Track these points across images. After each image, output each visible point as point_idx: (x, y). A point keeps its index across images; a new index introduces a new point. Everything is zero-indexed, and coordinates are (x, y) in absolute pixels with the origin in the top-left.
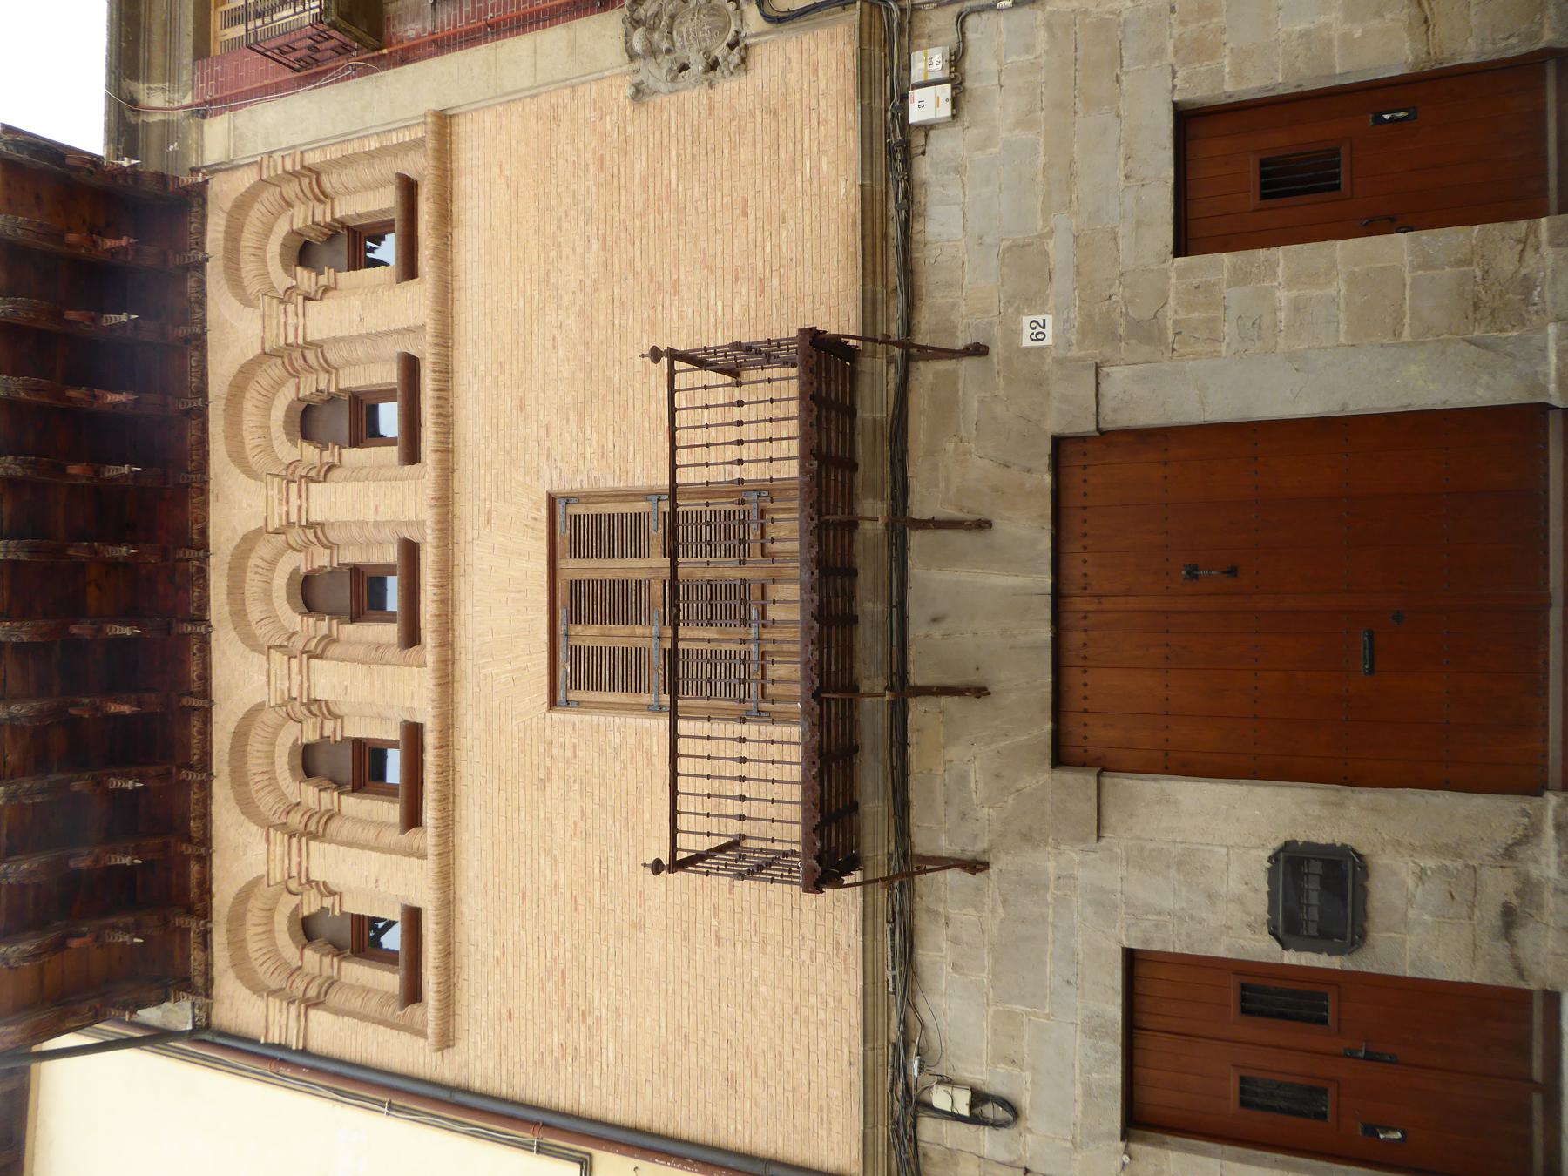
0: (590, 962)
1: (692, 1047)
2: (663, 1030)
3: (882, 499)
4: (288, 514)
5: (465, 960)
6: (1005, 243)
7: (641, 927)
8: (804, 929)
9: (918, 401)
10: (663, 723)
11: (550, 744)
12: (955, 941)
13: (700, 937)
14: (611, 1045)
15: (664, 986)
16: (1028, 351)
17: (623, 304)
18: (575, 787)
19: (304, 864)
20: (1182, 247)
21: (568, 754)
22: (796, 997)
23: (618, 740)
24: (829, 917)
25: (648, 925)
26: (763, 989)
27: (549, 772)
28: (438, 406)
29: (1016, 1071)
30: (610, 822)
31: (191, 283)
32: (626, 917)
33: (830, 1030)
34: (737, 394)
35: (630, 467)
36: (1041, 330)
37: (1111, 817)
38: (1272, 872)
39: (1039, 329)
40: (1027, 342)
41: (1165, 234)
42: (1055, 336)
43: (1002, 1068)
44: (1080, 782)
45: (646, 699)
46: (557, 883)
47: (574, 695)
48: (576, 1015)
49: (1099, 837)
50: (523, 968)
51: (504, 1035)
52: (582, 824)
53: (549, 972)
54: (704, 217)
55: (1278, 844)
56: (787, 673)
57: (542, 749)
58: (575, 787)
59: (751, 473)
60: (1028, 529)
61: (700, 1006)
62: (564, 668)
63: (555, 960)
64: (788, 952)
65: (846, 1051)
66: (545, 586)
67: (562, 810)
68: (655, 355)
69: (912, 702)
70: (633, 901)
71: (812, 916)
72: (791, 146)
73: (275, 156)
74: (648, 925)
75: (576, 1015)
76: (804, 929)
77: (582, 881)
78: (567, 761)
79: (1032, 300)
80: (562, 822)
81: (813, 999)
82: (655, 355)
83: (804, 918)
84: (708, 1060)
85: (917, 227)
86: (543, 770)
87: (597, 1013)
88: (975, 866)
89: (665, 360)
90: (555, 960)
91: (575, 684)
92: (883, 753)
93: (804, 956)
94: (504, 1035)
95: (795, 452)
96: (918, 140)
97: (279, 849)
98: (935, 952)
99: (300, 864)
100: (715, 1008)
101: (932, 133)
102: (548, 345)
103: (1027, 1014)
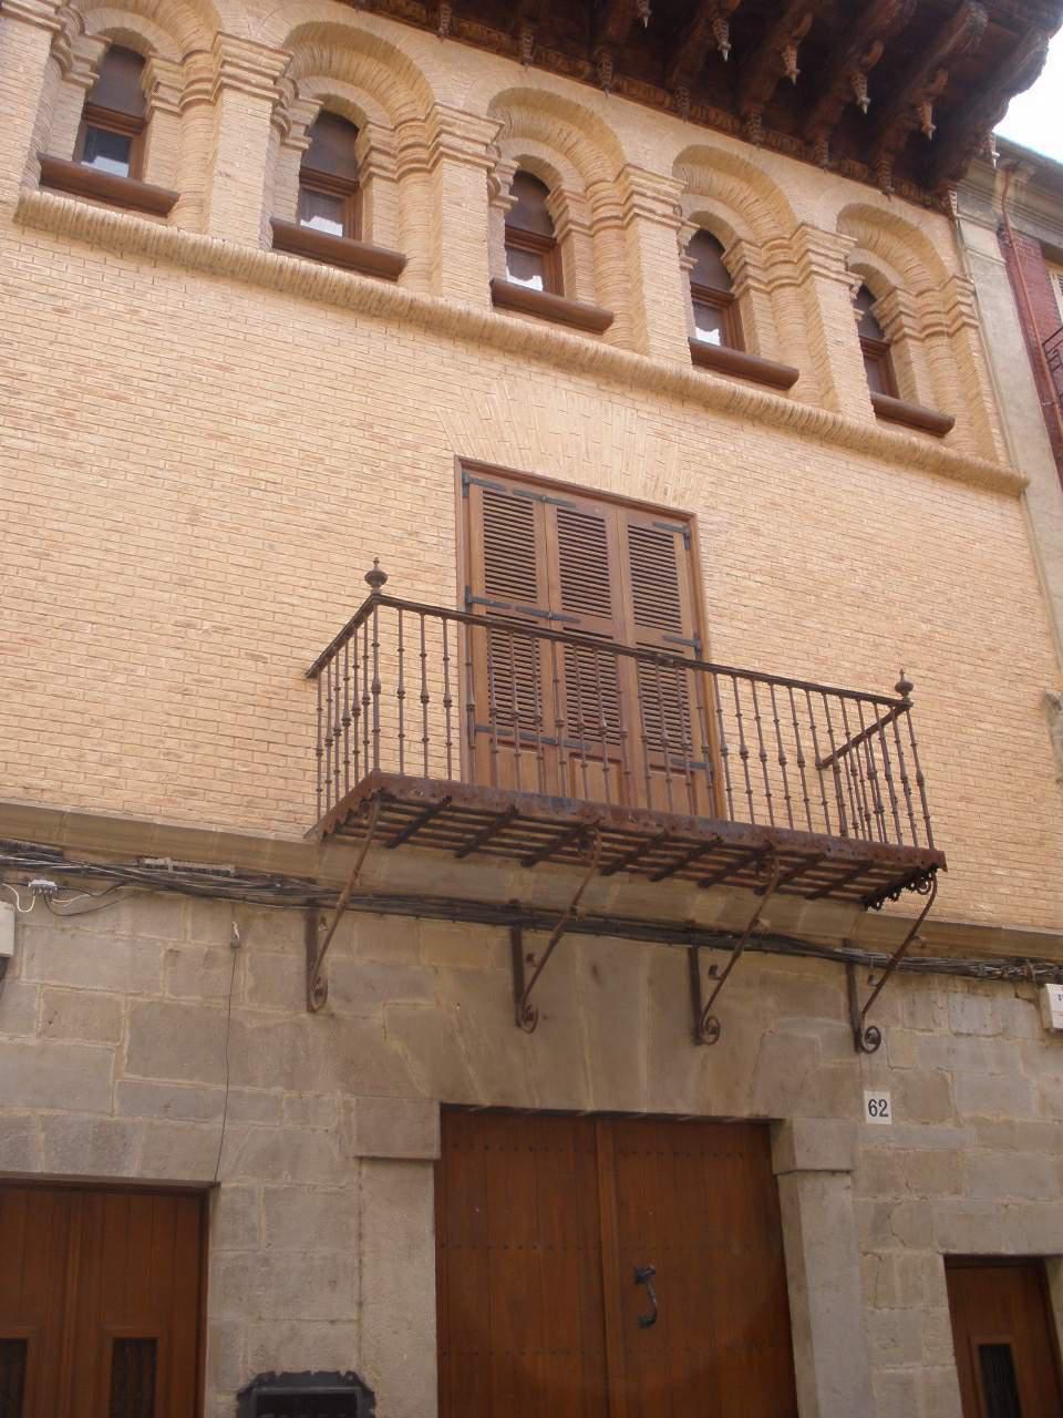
0: (140, 439)
1: (34, 562)
2: (55, 525)
3: (719, 920)
4: (643, 195)
5: (133, 267)
6: (949, 1076)
7: (192, 522)
8: (208, 749)
9: (812, 968)
10: (451, 602)
11: (416, 448)
12: (209, 958)
13: (185, 601)
14: (28, 445)
15: (115, 537)
16: (861, 1097)
17: (876, 645)
18: (366, 470)
19: (247, 88)
20: (954, 1264)
21: (407, 470)
22: (114, 724)
23: (427, 539)
24: (226, 787)
25: (197, 531)
26: (121, 679)
27: (383, 440)
28: (777, 408)
29: (39, 1025)
30: (327, 507)
31: (858, 166)
32: (204, 503)
33: (73, 766)
34: (809, 763)
35: (725, 620)
36: (879, 1109)
37: (387, 1176)
38: (335, 1377)
39: (880, 1109)
40: (868, 1095)
41: (962, 1248)
42: (875, 1126)
43: (39, 1005)
44: (425, 1136)
45: (479, 590)
46: (240, 416)
47: (476, 491)
48: (68, 404)
49: (361, 1159)
50: (126, 344)
51: (34, 295)
52: (320, 468)
53: (126, 380)
54: (956, 752)
55: (369, 1379)
56: (525, 777)
57: (409, 437)
58: (366, 470)
59: (735, 764)
60: (689, 1089)
61: (92, 584)
62: (511, 487)
63: (142, 391)
64: (175, 721)
65: (45, 784)
66: (605, 489)
67: (336, 445)
68: (904, 688)
69: (503, 933)
70: (227, 516)
71: (226, 763)
72: (1017, 857)
73: (972, 298)
74: (197, 531)
75: (68, 404)
76: (208, 749)
77: (247, 452)
78: (397, 467)
79: (905, 1101)
80: (322, 442)
81: (113, 748)
82: (904, 688)
83: (222, 751)
84: (17, 581)
85: (959, 983)
86: (384, 432)
87: (73, 435)
88: (316, 991)
89: (898, 697)
90: (142, 391)
91: (490, 496)
92: (443, 889)
93: (170, 743)
94: (34, 295)
95: (760, 821)
96: (1026, 992)
97: (264, 60)
98: (193, 932)
99: (246, 82)
100: (90, 605)
101: (1032, 1007)
102: (835, 551)
103: (120, 1048)
